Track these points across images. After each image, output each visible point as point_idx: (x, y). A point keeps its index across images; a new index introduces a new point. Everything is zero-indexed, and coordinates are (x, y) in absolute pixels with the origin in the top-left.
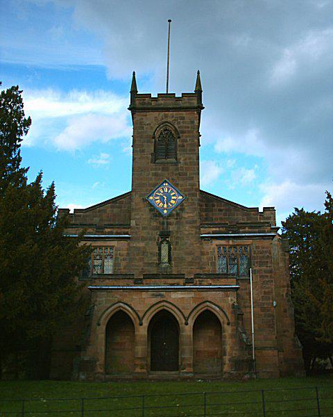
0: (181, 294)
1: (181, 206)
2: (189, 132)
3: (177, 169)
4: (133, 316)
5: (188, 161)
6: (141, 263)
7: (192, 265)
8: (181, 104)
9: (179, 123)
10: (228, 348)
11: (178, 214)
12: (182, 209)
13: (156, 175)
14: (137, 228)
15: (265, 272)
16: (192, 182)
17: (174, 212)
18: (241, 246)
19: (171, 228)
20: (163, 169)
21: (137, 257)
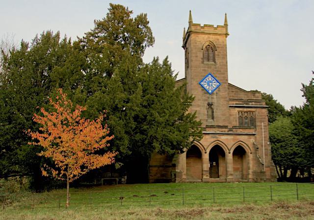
3: (216, 68)
4: (201, 148)
5: (221, 64)
10: (251, 166)
11: (217, 93)
13: (205, 70)
16: (223, 76)
20: (208, 68)
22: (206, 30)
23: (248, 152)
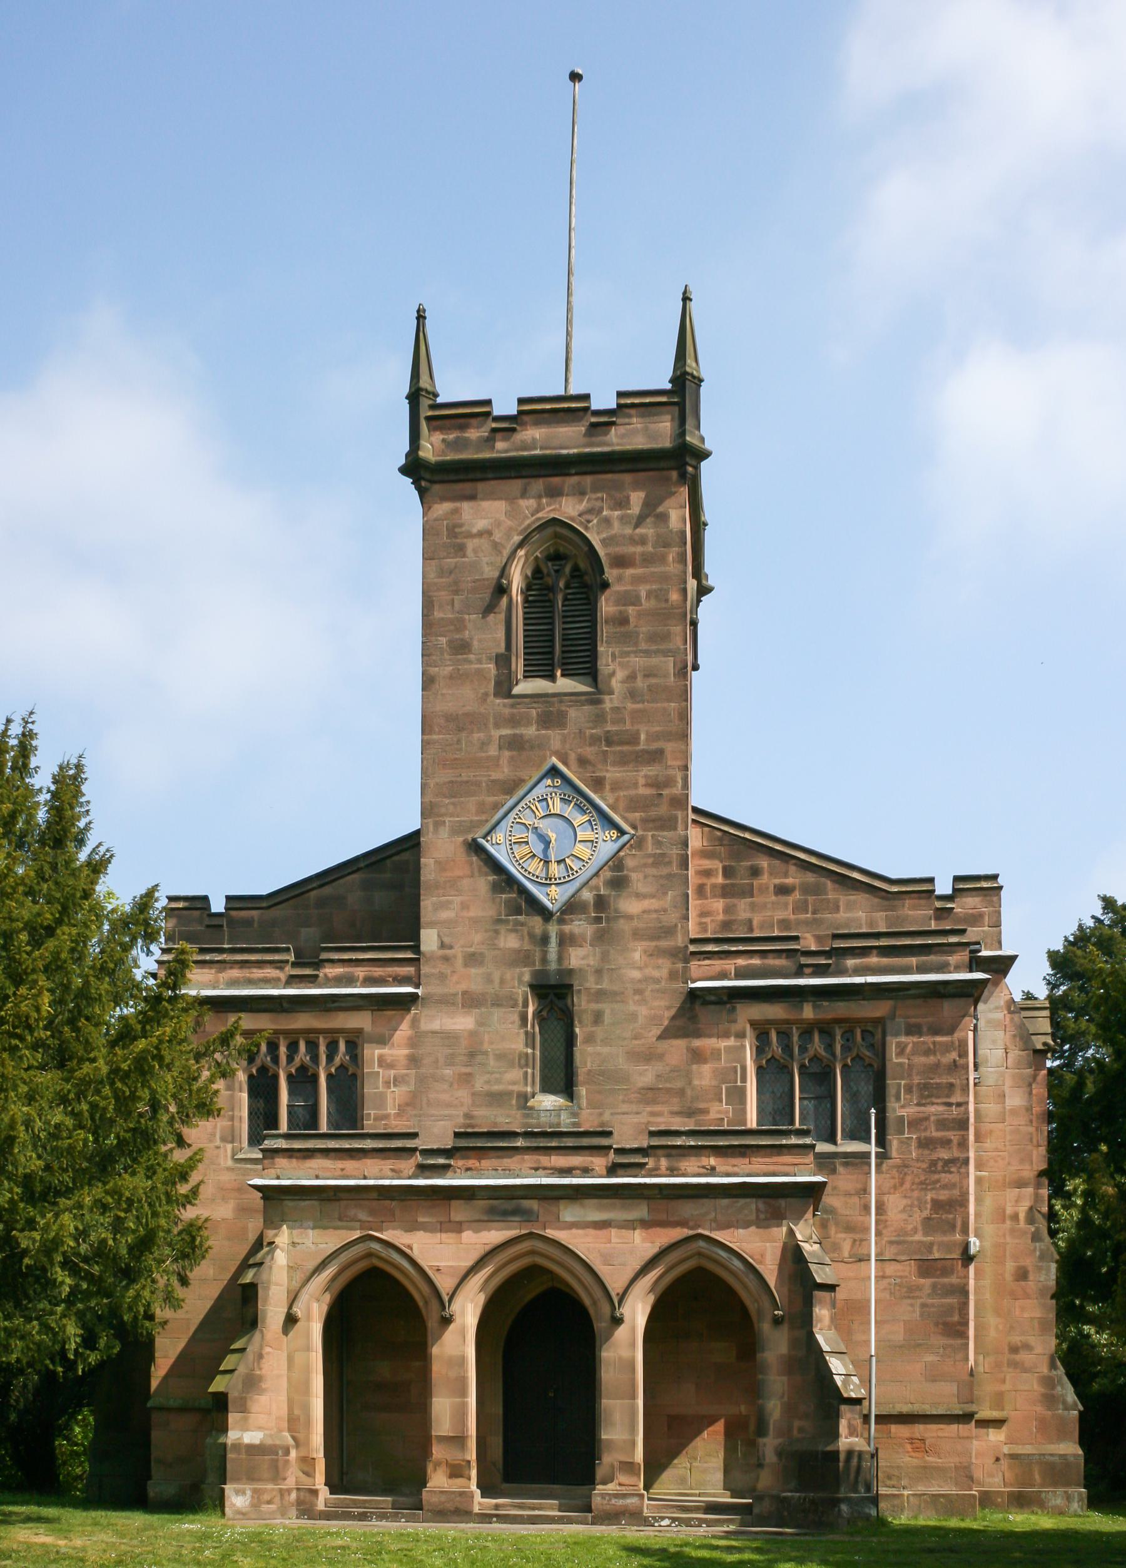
0: (600, 1208)
1: (616, 874)
2: (648, 560)
5: (640, 683)
6: (463, 1094)
7: (654, 1101)
8: (617, 440)
9: (607, 521)
10: (774, 1408)
11: (601, 903)
12: (619, 883)
13: (515, 744)
14: (446, 959)
15: (942, 1124)
17: (587, 895)
18: (849, 1024)
19: (577, 958)
21: (448, 1072)
22: (536, 439)
23: (760, 1312)
